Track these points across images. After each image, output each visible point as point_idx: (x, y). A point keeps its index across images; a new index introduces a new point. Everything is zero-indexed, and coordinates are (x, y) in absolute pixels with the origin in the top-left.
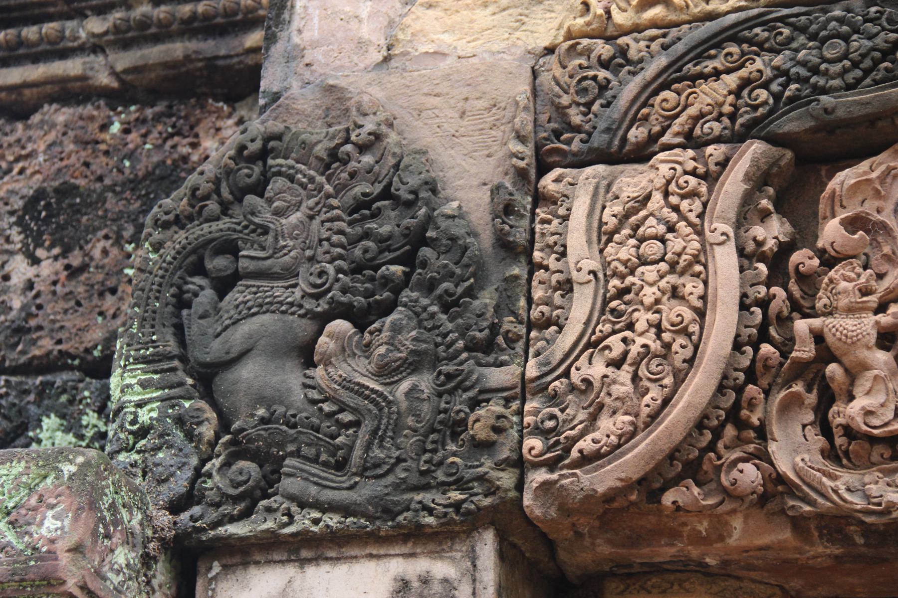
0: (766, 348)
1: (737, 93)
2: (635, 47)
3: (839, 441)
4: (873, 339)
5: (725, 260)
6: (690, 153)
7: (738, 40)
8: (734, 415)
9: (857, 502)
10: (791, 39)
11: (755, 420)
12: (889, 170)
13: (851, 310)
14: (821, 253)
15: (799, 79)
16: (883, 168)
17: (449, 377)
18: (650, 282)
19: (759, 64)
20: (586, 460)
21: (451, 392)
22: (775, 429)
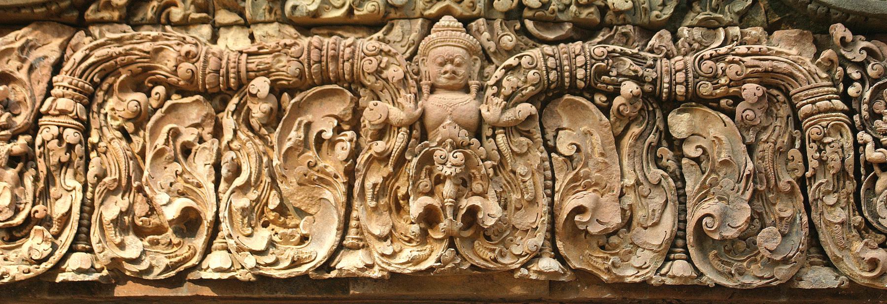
12: (28, 41)
16: (23, 41)
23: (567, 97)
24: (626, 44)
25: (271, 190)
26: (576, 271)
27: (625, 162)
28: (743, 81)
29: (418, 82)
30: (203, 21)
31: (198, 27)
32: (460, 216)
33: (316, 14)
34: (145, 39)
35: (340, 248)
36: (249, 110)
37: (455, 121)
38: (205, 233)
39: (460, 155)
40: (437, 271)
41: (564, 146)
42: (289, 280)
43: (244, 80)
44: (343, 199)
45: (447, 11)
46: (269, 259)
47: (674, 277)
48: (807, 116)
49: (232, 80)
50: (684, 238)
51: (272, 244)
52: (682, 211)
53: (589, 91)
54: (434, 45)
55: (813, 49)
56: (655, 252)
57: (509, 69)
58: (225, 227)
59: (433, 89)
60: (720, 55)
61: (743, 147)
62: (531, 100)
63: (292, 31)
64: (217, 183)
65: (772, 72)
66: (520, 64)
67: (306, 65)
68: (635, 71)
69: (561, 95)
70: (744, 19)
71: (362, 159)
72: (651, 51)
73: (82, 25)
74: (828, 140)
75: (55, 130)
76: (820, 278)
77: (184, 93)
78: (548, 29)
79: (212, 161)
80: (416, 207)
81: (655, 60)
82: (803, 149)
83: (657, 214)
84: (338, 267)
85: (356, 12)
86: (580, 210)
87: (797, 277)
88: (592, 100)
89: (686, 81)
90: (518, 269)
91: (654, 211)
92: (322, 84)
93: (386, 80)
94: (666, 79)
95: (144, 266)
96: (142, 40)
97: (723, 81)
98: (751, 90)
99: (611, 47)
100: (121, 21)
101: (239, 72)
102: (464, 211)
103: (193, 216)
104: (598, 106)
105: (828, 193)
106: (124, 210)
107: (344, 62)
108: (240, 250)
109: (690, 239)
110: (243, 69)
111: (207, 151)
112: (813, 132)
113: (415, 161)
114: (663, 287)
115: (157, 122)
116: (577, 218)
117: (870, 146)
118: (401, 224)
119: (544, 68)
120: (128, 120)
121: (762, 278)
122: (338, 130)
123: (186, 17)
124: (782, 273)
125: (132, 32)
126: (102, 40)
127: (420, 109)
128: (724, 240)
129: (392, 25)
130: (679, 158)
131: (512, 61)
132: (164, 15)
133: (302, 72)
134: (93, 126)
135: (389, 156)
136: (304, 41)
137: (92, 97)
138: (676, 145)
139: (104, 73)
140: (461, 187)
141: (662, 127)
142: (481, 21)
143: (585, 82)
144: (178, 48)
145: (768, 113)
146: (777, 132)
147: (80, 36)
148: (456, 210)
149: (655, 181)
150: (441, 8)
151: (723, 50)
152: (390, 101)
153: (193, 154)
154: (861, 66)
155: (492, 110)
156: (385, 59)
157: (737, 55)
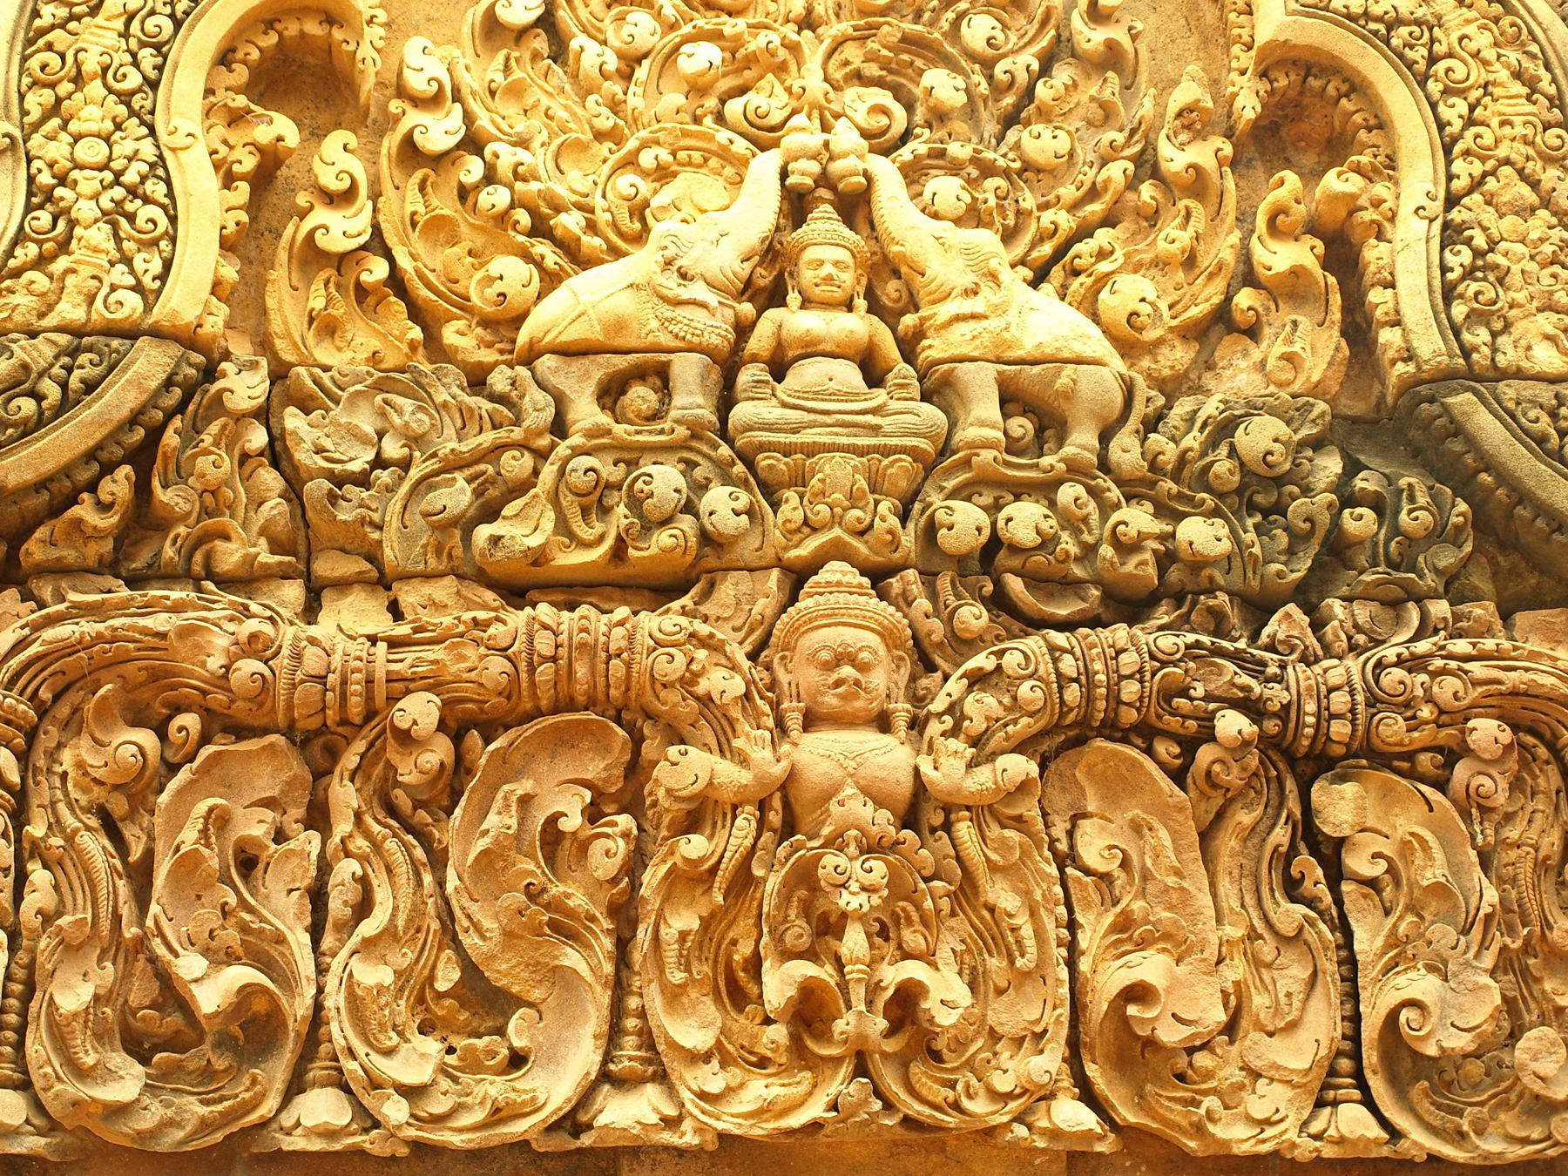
23: (1100, 743)
24: (1217, 633)
25: (440, 949)
27: (1226, 886)
29: (775, 706)
31: (273, 584)
32: (880, 1005)
33: (538, 557)
36: (391, 767)
37: (865, 791)
38: (290, 1045)
39: (879, 867)
40: (828, 1129)
43: (380, 699)
44: (608, 968)
45: (836, 552)
46: (438, 1105)
47: (1341, 1141)
49: (354, 700)
50: (1356, 1056)
51: (443, 1070)
53: (1145, 734)
54: (811, 623)
56: (1294, 1087)
57: (978, 680)
58: (340, 1031)
59: (810, 721)
60: (1414, 657)
61: (1473, 854)
62: (1022, 747)
63: (489, 596)
64: (316, 932)
66: (999, 668)
67: (523, 666)
68: (1243, 688)
69: (1080, 741)
71: (652, 877)
72: (1271, 648)
77: (241, 732)
78: (1050, 597)
79: (307, 882)
80: (779, 983)
81: (1283, 667)
83: (1296, 1003)
84: (601, 1120)
85: (632, 552)
86: (1138, 993)
88: (1149, 751)
89: (1352, 711)
90: (1007, 1126)
91: (1289, 995)
92: (555, 711)
93: (706, 700)
94: (1311, 707)
96: (149, 608)
98: (1486, 731)
99: (1191, 638)
101: (370, 681)
102: (890, 992)
103: (260, 1006)
104: (1162, 766)
106: (102, 992)
107: (609, 658)
108: (375, 1084)
110: (380, 674)
111: (296, 861)
113: (773, 882)
115: (180, 792)
116: (1132, 1010)
118: (743, 1023)
119: (1053, 677)
120: (116, 787)
121: (1525, 1141)
122: (593, 814)
123: (250, 560)
125: (125, 593)
126: (62, 607)
127: (784, 763)
129: (712, 585)
130: (1335, 874)
132: (198, 557)
133: (515, 679)
134: (34, 802)
135: (713, 871)
136: (517, 619)
137: (31, 735)
138: (1331, 853)
139: (61, 681)
140: (878, 941)
141: (1298, 813)
142: (911, 574)
143: (1139, 710)
144: (231, 627)
145: (1516, 785)
148: (874, 989)
149: (1288, 929)
150: (822, 546)
151: (1423, 647)
152: (715, 747)
153: (261, 866)
155: (949, 768)
156: (701, 654)
157: (1450, 657)
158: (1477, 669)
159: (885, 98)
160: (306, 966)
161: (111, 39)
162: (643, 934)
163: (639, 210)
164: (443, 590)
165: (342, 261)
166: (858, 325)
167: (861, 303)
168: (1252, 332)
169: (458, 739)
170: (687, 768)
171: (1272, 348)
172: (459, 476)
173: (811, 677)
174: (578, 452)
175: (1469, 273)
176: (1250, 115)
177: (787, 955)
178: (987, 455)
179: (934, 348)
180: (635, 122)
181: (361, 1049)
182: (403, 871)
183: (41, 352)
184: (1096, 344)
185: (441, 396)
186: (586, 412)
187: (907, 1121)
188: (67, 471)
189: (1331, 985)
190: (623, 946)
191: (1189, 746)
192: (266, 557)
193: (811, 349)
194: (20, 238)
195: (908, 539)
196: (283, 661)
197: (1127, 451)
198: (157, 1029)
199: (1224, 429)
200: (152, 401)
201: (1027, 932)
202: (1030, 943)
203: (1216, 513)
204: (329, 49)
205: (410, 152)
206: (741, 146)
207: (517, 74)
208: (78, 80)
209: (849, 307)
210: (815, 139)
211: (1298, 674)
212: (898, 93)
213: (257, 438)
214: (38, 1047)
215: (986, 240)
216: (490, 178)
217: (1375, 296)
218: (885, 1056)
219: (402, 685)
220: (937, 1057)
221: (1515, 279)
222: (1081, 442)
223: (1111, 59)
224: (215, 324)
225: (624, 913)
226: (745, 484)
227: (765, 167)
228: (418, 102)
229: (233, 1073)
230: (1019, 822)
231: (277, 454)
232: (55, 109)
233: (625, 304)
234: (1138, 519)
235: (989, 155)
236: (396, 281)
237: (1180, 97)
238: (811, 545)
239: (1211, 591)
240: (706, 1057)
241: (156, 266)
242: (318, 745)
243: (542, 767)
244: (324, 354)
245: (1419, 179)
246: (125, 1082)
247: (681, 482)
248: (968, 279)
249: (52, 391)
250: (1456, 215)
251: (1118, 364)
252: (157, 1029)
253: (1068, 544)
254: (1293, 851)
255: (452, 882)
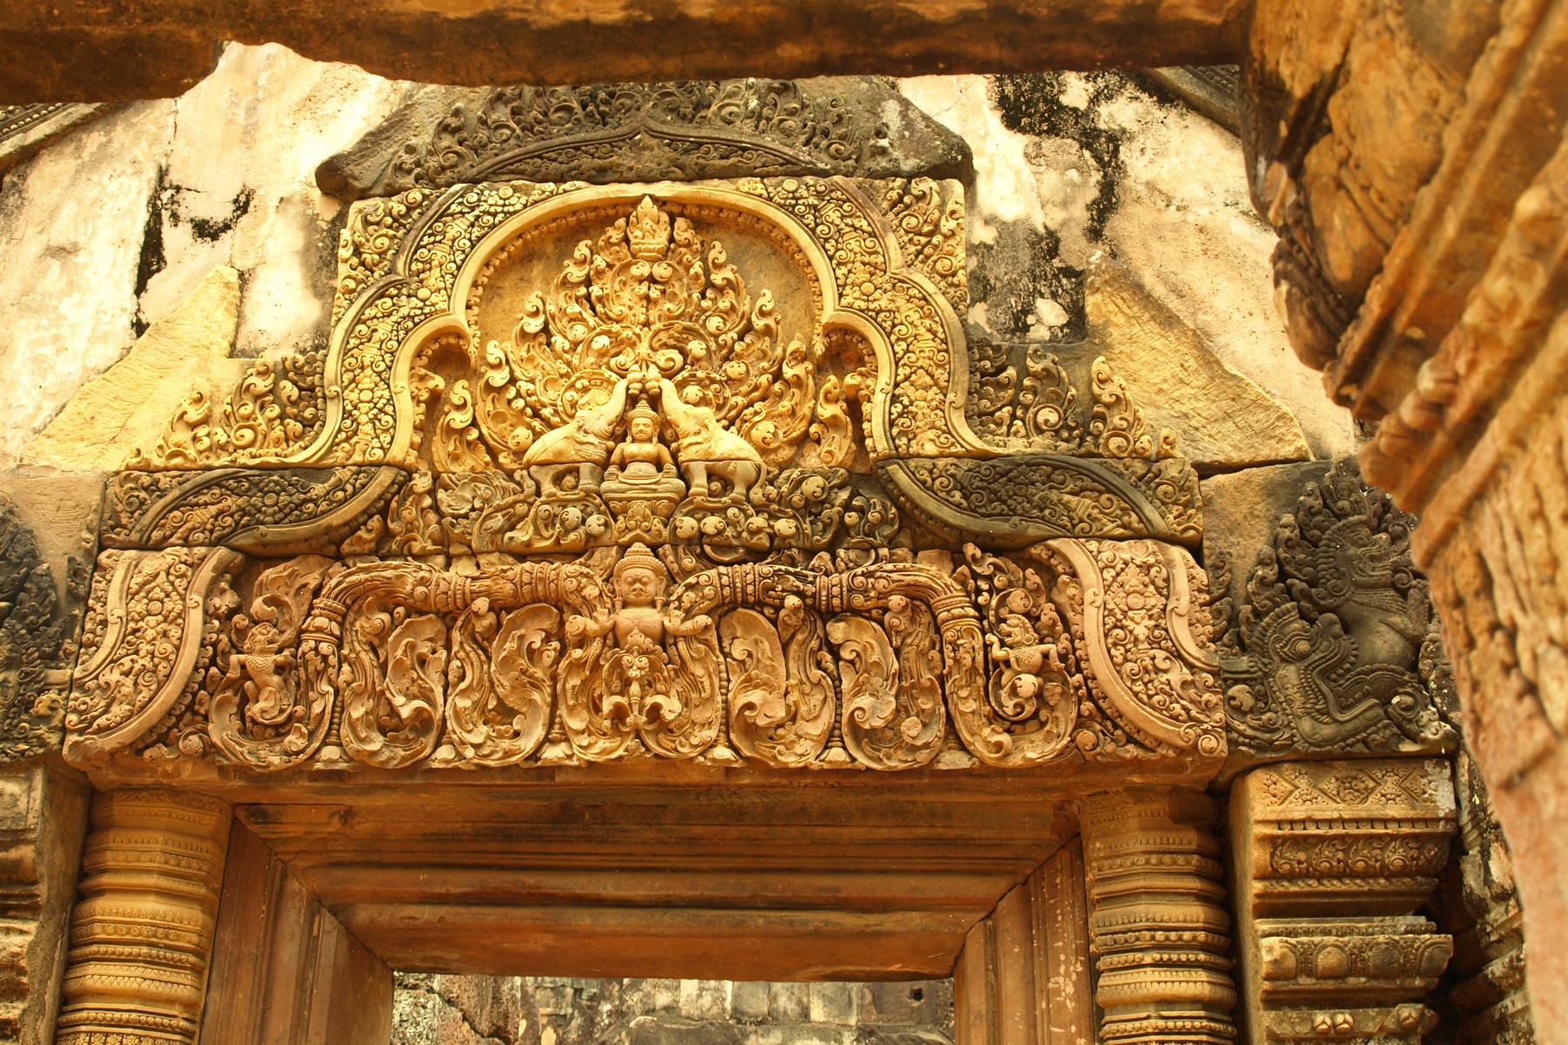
0: (214, 670)
1: (216, 517)
2: (164, 480)
3: (249, 725)
4: (271, 669)
5: (195, 617)
6: (185, 550)
7: (220, 486)
8: (190, 708)
9: (253, 760)
10: (249, 490)
11: (202, 711)
13: (263, 652)
14: (250, 616)
15: (249, 514)
17: (27, 674)
18: (151, 626)
19: (229, 502)
20: (100, 730)
21: (28, 684)
22: (213, 716)
26: (746, 759)
27: (792, 664)
28: (891, 593)
30: (438, 553)
33: (528, 544)
34: (388, 571)
35: (547, 740)
37: (642, 631)
41: (738, 651)
42: (503, 769)
46: (486, 751)
48: (944, 622)
51: (489, 737)
52: (839, 706)
53: (759, 605)
55: (951, 566)
57: (689, 587)
59: (625, 605)
63: (510, 559)
65: (916, 585)
70: (892, 543)
71: (563, 664)
73: (339, 557)
74: (960, 642)
75: (312, 644)
76: (954, 760)
77: (421, 613)
78: (724, 553)
80: (607, 705)
82: (941, 651)
86: (750, 706)
87: (935, 759)
88: (762, 613)
95: (383, 757)
96: (387, 568)
97: (872, 594)
98: (896, 600)
99: (777, 567)
100: (371, 553)
103: (425, 715)
105: (961, 687)
108: (463, 743)
109: (845, 729)
112: (949, 635)
114: (822, 771)
117: (996, 646)
118: (597, 719)
122: (547, 640)
124: (923, 757)
128: (873, 729)
130: (837, 658)
131: (692, 580)
133: (516, 591)
136: (518, 568)
137: (344, 616)
138: (834, 651)
142: (667, 546)
145: (912, 620)
146: (920, 638)
147: (337, 566)
149: (815, 681)
151: (873, 568)
154: (989, 578)
155: (674, 621)
156: (584, 580)
158: (895, 576)
159: (675, 354)
160: (440, 700)
161: (375, 351)
162: (559, 687)
163: (574, 405)
164: (494, 558)
165: (462, 432)
166: (650, 448)
167: (655, 439)
168: (818, 442)
169: (498, 616)
170: (576, 624)
171: (824, 448)
172: (500, 515)
173: (625, 588)
174: (543, 503)
175: (900, 415)
176: (819, 353)
177: (613, 694)
178: (699, 499)
179: (682, 457)
180: (575, 369)
181: (458, 730)
182: (476, 663)
183: (344, 474)
184: (747, 450)
185: (496, 483)
186: (548, 487)
187: (656, 755)
188: (355, 518)
189: (831, 704)
190: (554, 687)
191: (778, 609)
192: (430, 547)
193: (635, 459)
194: (340, 431)
195: (666, 533)
196: (432, 587)
197: (757, 494)
198: (389, 724)
199: (799, 483)
200: (387, 490)
201: (707, 683)
202: (708, 688)
203: (794, 517)
204: (460, 347)
205: (489, 388)
206: (614, 377)
207: (532, 352)
208: (363, 368)
209: (650, 440)
210: (639, 375)
211: (823, 580)
212: (683, 352)
213: (427, 501)
214: (345, 731)
215: (706, 412)
216: (519, 395)
217: (865, 426)
218: (647, 732)
219: (476, 595)
220: (671, 731)
221: (920, 416)
222: (739, 491)
223: (768, 331)
224: (412, 458)
225: (554, 678)
226: (604, 513)
227: (622, 384)
228: (493, 367)
229: (415, 740)
230: (706, 642)
231: (435, 507)
232: (353, 381)
233: (562, 445)
234: (759, 521)
235: (713, 375)
236: (481, 438)
237: (792, 347)
238: (629, 536)
239: (789, 548)
240: (583, 732)
241: (388, 439)
242: (447, 617)
243: (528, 624)
244: (453, 469)
245: (884, 378)
246: (377, 743)
247: (579, 514)
248: (697, 428)
249: (349, 488)
250: (897, 392)
251: (757, 458)
252: (389, 724)
253: (729, 532)
254: (820, 649)
255: (493, 668)
